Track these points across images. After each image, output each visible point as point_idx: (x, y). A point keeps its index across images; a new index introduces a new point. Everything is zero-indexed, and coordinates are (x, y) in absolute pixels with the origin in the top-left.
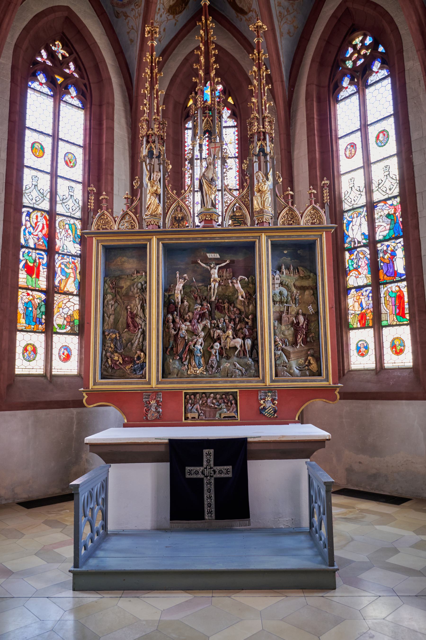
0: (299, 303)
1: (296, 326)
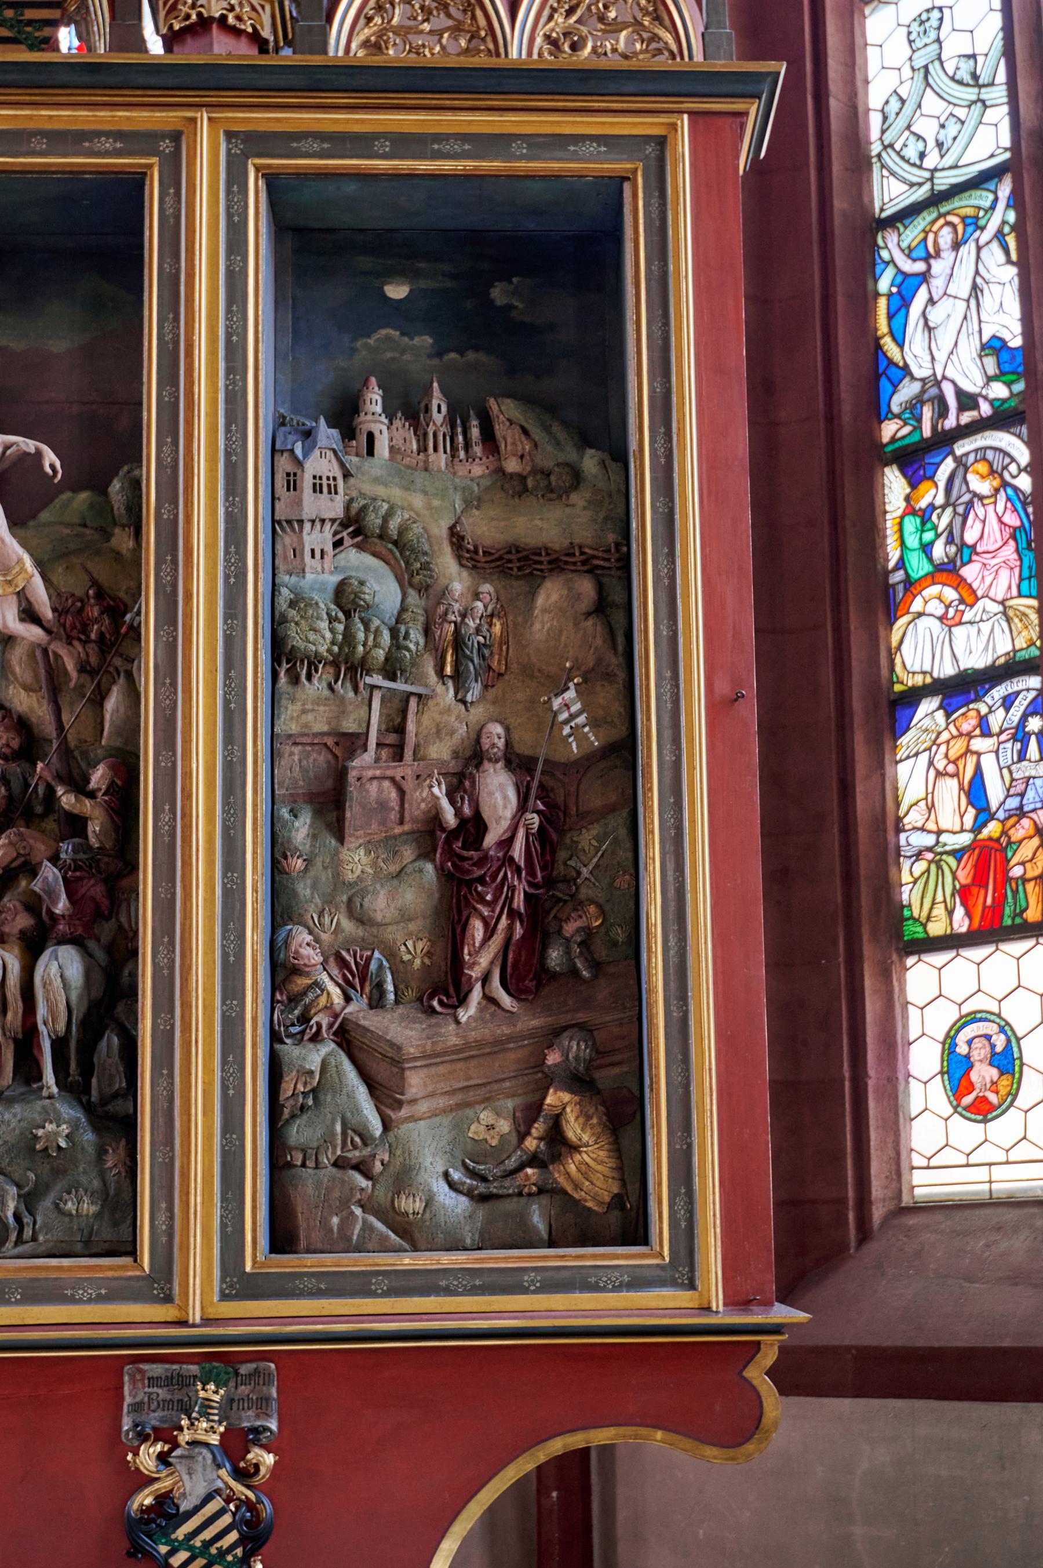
0: (491, 678)
1: (455, 848)
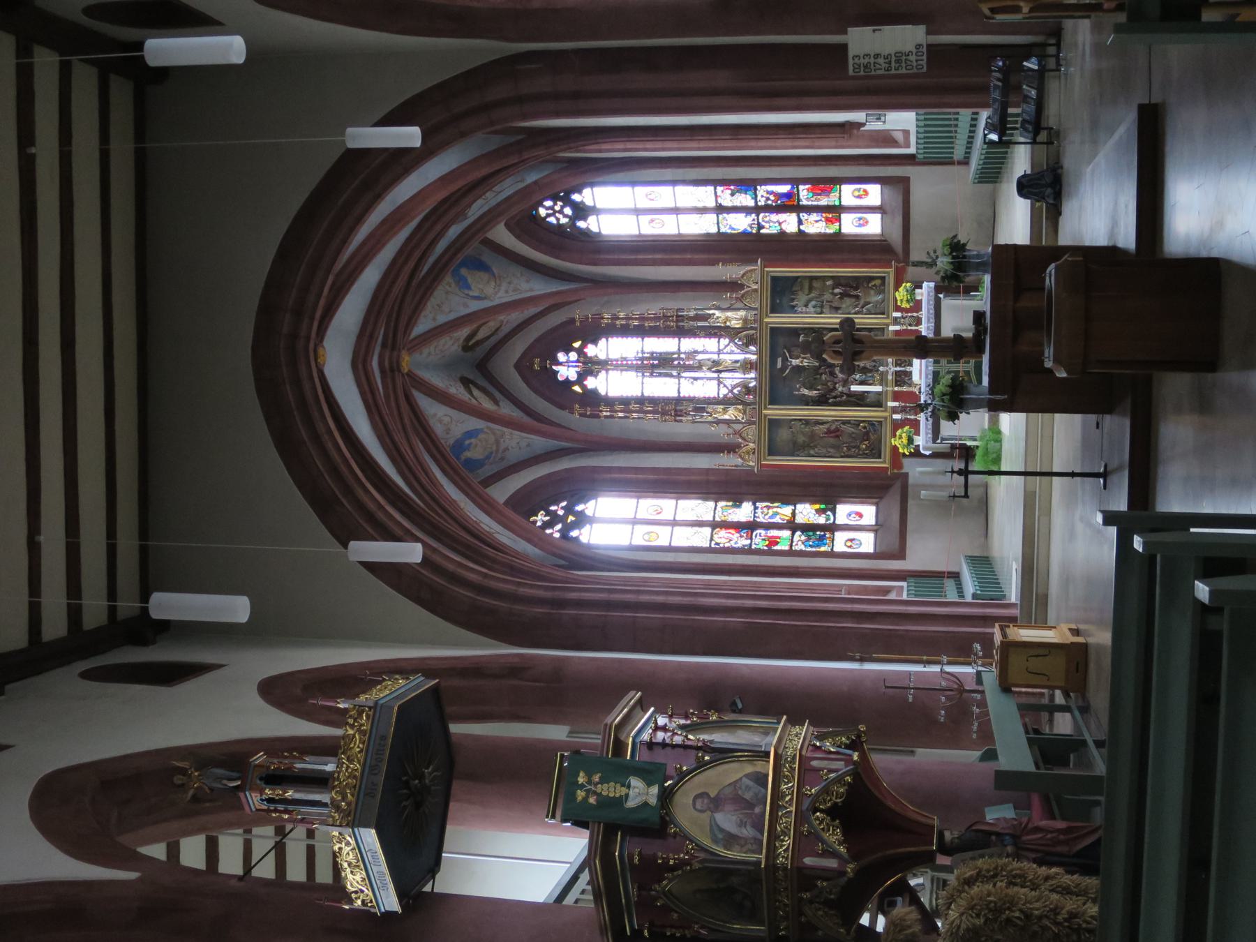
1: (843, 295)
